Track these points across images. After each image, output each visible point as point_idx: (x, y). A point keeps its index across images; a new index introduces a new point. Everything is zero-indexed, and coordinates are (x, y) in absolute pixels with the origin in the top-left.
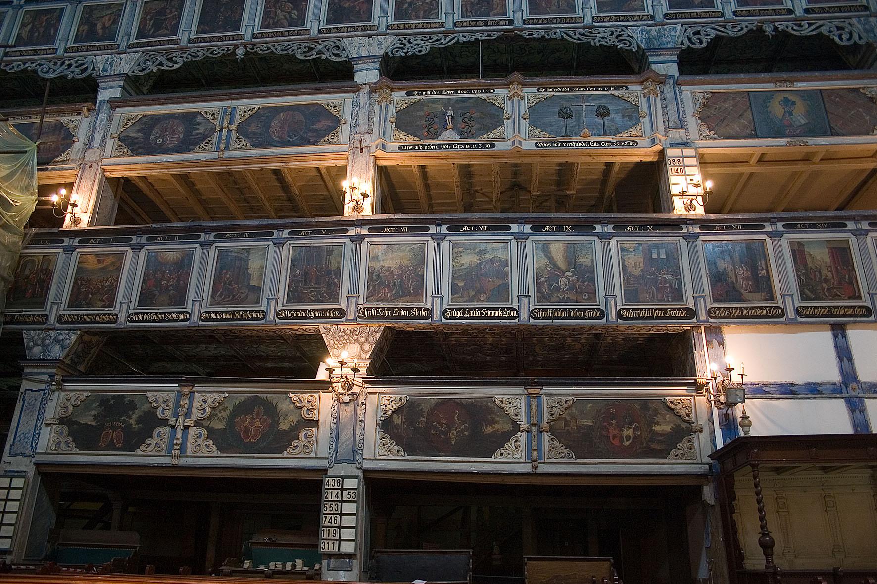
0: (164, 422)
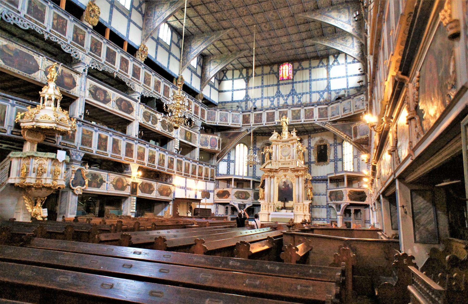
0: (105, 182)
